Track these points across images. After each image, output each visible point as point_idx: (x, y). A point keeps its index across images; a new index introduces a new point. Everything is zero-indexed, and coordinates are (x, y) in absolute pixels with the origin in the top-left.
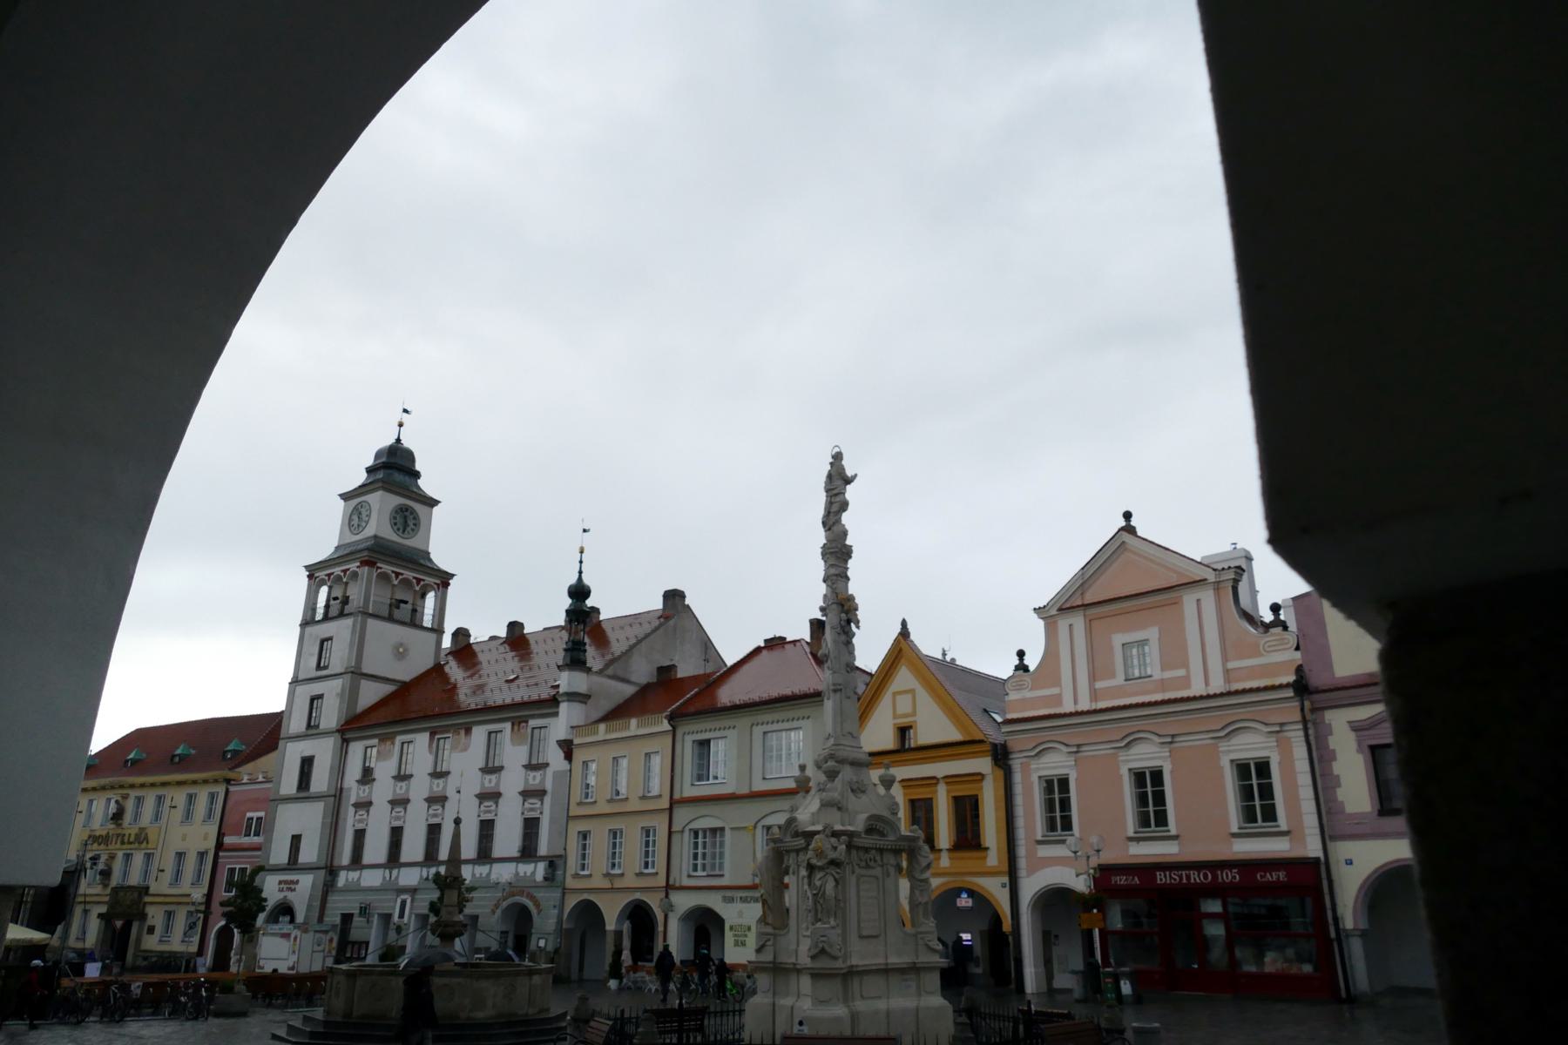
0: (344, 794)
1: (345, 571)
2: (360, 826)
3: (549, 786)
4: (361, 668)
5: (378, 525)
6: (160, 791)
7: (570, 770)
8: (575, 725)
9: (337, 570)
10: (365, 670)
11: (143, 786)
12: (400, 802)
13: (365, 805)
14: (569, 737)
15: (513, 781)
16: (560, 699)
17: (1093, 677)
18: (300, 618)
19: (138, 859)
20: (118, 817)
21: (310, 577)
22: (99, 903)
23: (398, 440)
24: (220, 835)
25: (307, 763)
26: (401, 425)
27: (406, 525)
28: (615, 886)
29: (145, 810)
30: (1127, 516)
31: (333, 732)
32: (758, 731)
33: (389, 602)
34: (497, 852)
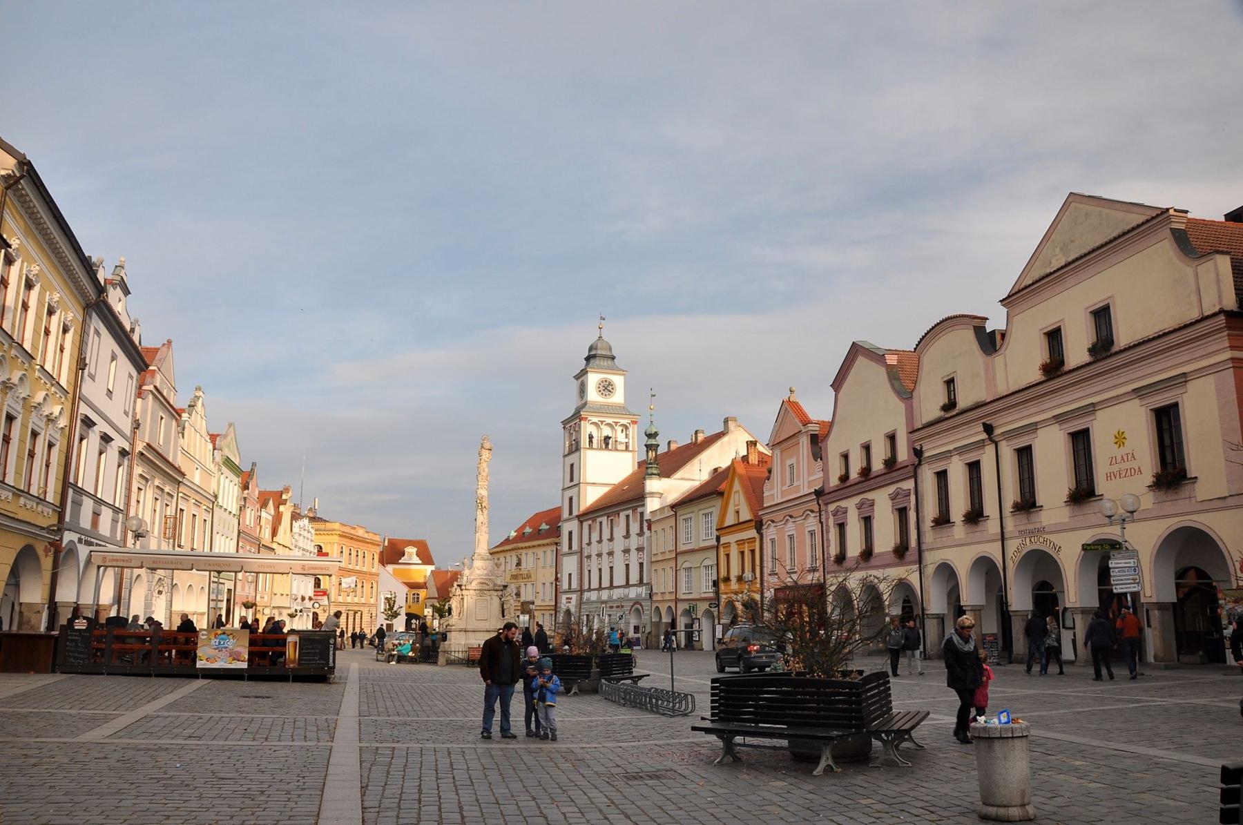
1: (575, 424)
2: (589, 568)
6: (534, 550)
7: (651, 536)
9: (572, 423)
10: (589, 480)
11: (526, 548)
12: (600, 555)
13: (589, 557)
14: (650, 518)
15: (634, 542)
17: (782, 486)
19: (529, 585)
20: (519, 564)
21: (564, 428)
22: (518, 610)
24: (556, 573)
25: (570, 533)
26: (600, 328)
29: (528, 560)
34: (630, 583)
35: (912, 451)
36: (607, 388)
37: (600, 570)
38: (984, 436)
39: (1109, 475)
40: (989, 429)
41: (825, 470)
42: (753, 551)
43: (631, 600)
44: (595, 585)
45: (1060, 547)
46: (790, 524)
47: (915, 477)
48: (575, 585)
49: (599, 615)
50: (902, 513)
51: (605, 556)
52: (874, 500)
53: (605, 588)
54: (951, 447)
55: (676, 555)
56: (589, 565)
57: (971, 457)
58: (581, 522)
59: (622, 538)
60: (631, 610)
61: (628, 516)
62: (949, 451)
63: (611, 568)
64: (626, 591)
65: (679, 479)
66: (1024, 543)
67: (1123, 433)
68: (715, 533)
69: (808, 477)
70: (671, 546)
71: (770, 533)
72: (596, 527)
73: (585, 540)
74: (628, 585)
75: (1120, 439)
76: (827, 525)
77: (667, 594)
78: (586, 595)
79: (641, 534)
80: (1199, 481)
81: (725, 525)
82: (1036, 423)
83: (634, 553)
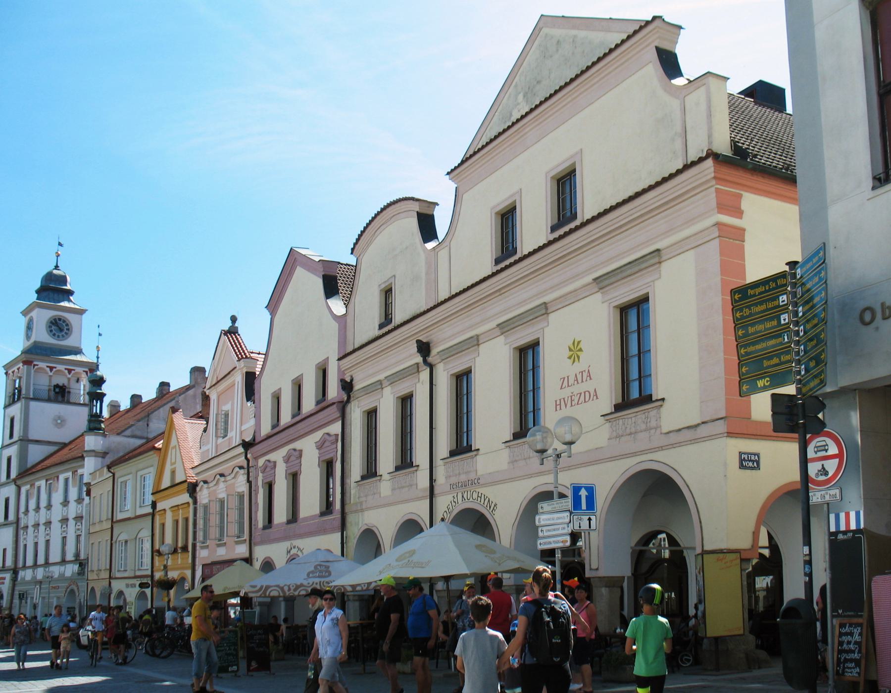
0: (20, 521)
3: (84, 514)
4: (28, 437)
5: (42, 335)
7: (90, 503)
8: (91, 472)
9: (15, 369)
12: (36, 526)
14: (89, 481)
15: (73, 509)
16: (84, 455)
18: (3, 404)
21: (6, 373)
23: (57, 267)
27: (61, 330)
28: (100, 578)
30: (234, 319)
31: (11, 482)
32: (140, 473)
33: (47, 388)
35: (340, 383)
36: (59, 326)
37: (36, 544)
38: (419, 359)
39: (558, 403)
40: (424, 348)
41: (257, 416)
42: (186, 520)
43: (67, 579)
44: (30, 562)
45: (495, 505)
46: (222, 485)
47: (343, 417)
48: (9, 563)
49: (32, 598)
50: (329, 466)
51: (42, 528)
52: (301, 451)
53: (41, 566)
54: (381, 377)
55: (112, 526)
56: (25, 539)
57: (403, 388)
58: (19, 488)
59: (61, 506)
60: (66, 592)
61: (67, 480)
62: (380, 382)
63: (48, 542)
64: (62, 568)
65: (129, 437)
66: (455, 500)
67: (579, 342)
68: (149, 499)
69: (241, 424)
70: (106, 514)
71: (203, 496)
72: (33, 493)
73: (22, 509)
74: (64, 562)
75: (575, 351)
76: (257, 485)
77: (102, 571)
78: (21, 574)
79: (80, 500)
80: (666, 404)
81: (163, 487)
82: (478, 336)
83: (71, 523)
